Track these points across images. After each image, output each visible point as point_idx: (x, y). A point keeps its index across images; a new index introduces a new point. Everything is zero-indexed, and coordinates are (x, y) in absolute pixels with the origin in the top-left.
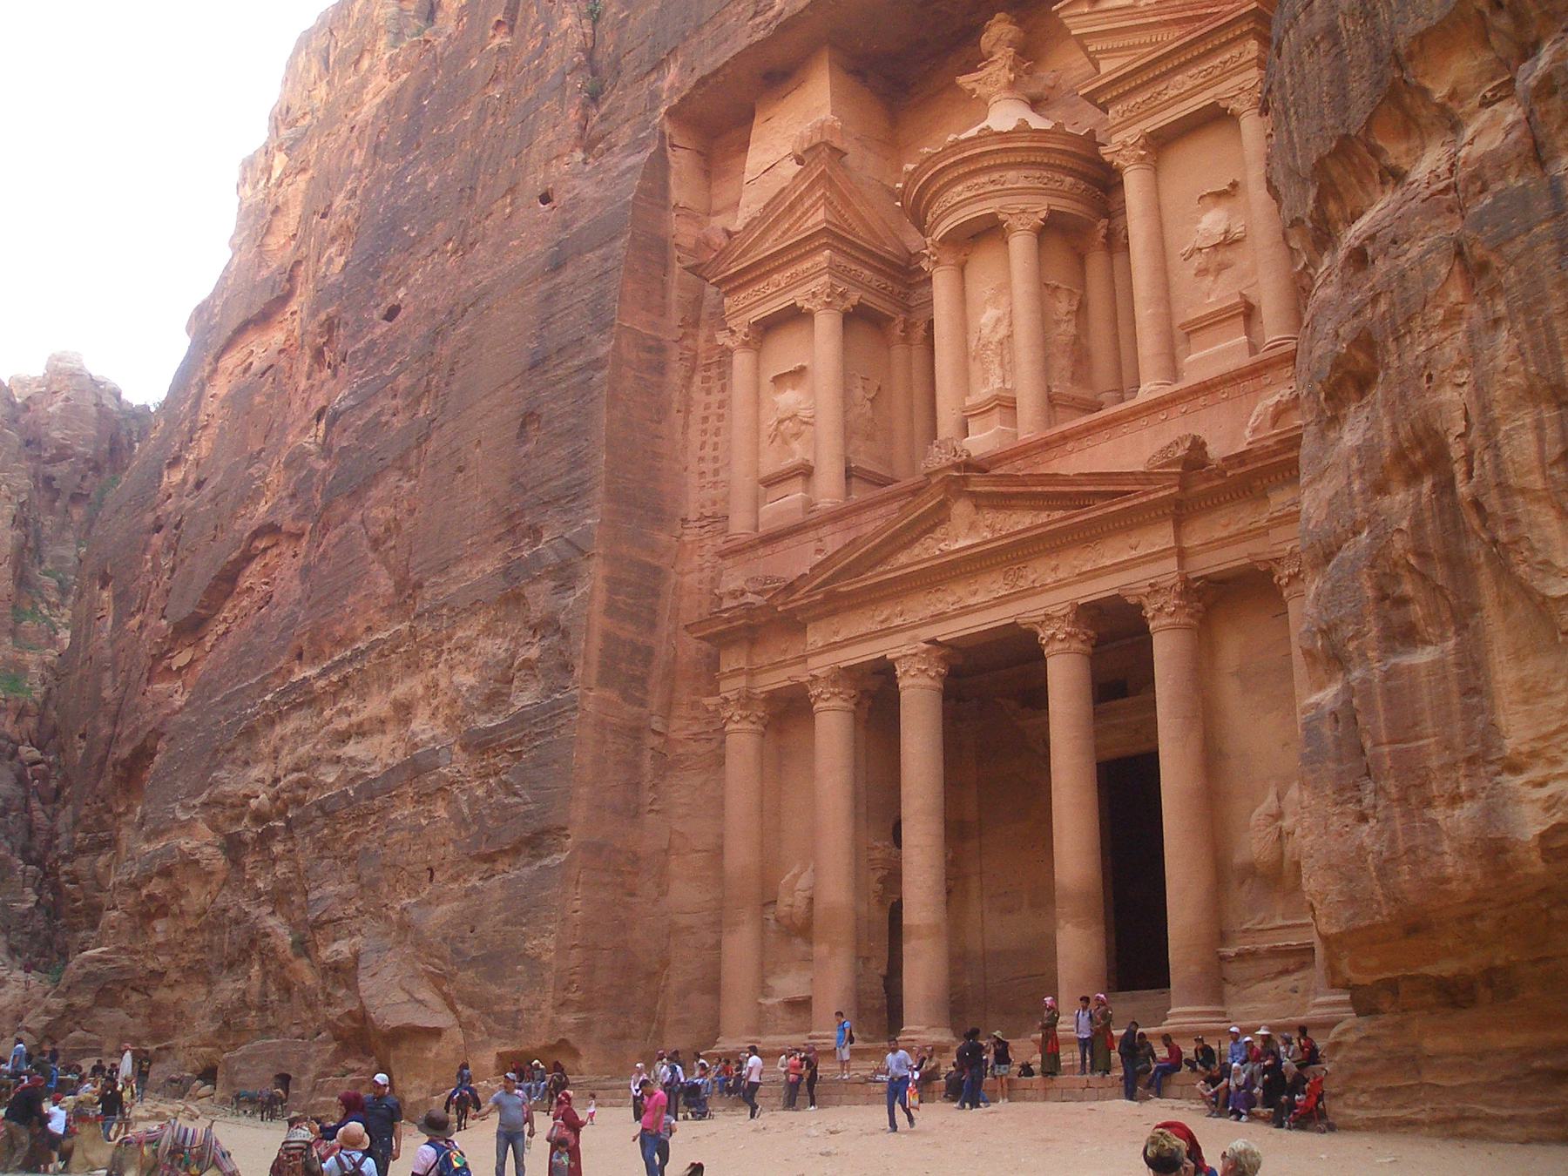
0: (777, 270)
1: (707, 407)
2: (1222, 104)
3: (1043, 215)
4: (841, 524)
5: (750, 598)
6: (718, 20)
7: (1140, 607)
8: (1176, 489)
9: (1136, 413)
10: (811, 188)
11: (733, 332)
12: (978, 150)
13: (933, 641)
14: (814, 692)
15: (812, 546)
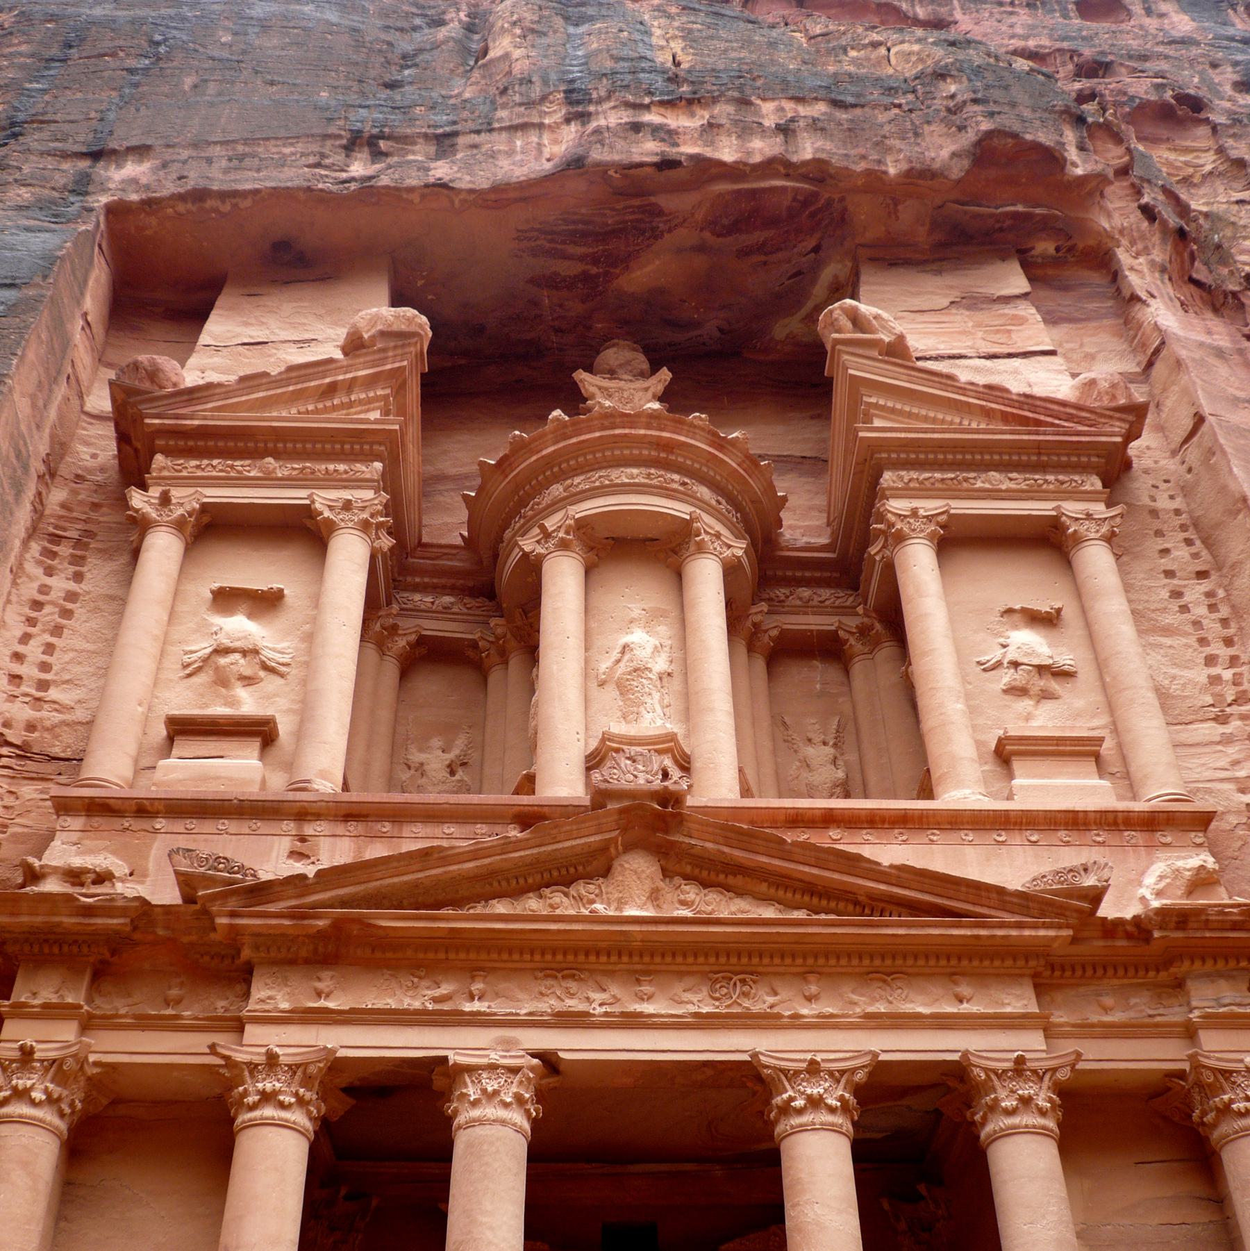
0: (277, 455)
1: (44, 589)
2: (1064, 518)
3: (740, 553)
4: (353, 827)
5: (119, 887)
6: (240, 148)
7: (987, 1087)
8: (1070, 932)
10: (371, 381)
11: (165, 500)
12: (683, 439)
13: (549, 1061)
14: (269, 1086)
15: (285, 844)
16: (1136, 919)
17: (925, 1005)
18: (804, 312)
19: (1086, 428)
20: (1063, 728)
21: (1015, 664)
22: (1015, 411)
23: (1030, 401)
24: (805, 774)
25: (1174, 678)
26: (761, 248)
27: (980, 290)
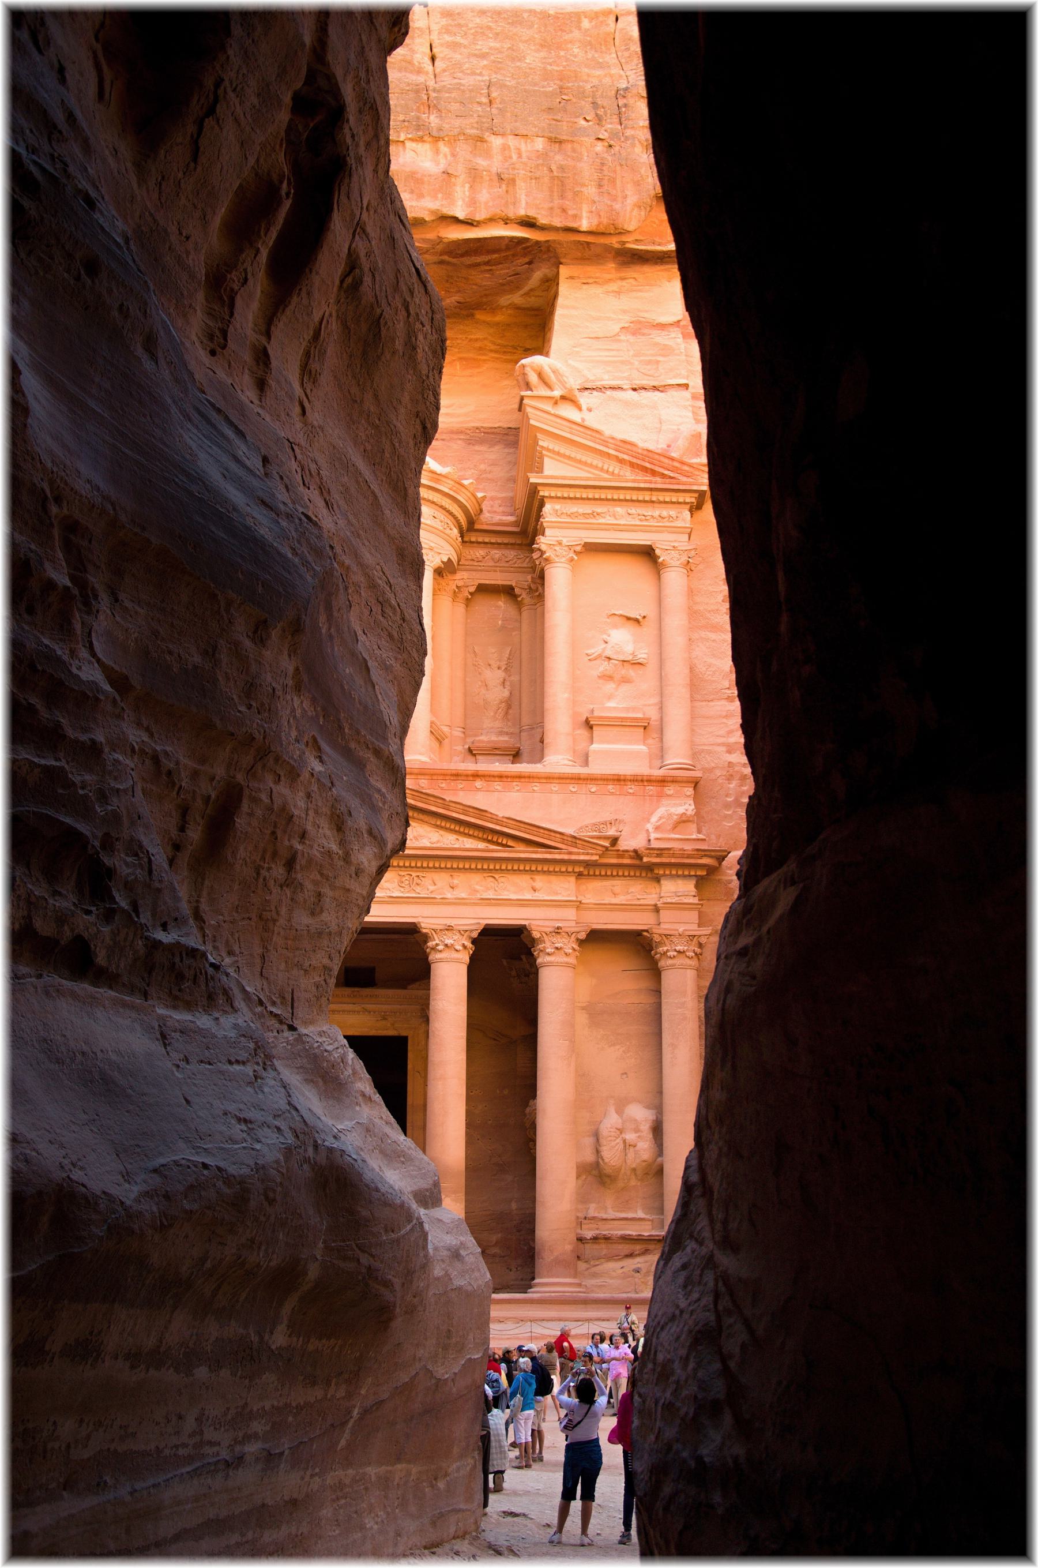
2: (658, 552)
3: (445, 560)
9: (549, 778)
16: (635, 851)
17: (515, 893)
18: (521, 292)
19: (685, 479)
20: (627, 709)
21: (609, 658)
22: (639, 462)
23: (650, 454)
24: (483, 691)
25: (710, 666)
26: (487, 263)
27: (646, 315)
